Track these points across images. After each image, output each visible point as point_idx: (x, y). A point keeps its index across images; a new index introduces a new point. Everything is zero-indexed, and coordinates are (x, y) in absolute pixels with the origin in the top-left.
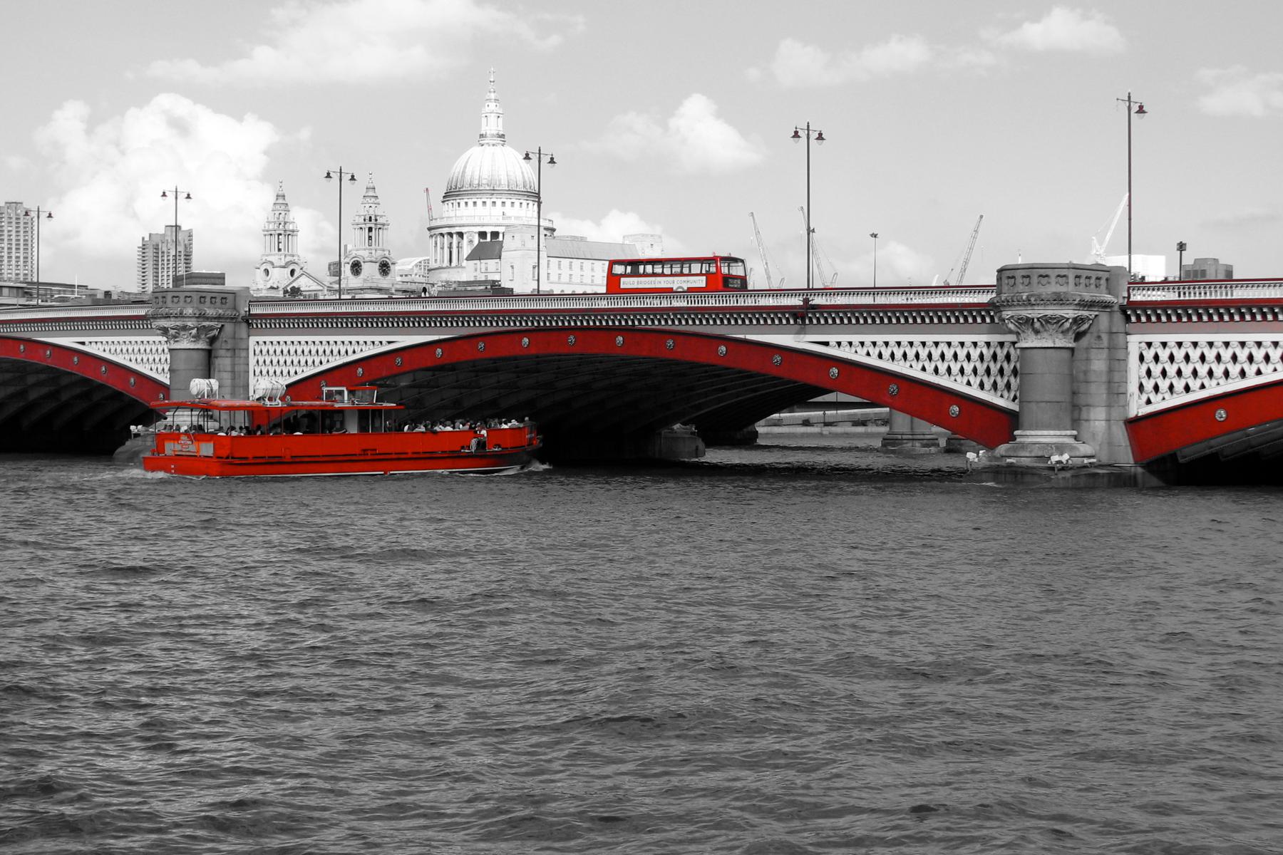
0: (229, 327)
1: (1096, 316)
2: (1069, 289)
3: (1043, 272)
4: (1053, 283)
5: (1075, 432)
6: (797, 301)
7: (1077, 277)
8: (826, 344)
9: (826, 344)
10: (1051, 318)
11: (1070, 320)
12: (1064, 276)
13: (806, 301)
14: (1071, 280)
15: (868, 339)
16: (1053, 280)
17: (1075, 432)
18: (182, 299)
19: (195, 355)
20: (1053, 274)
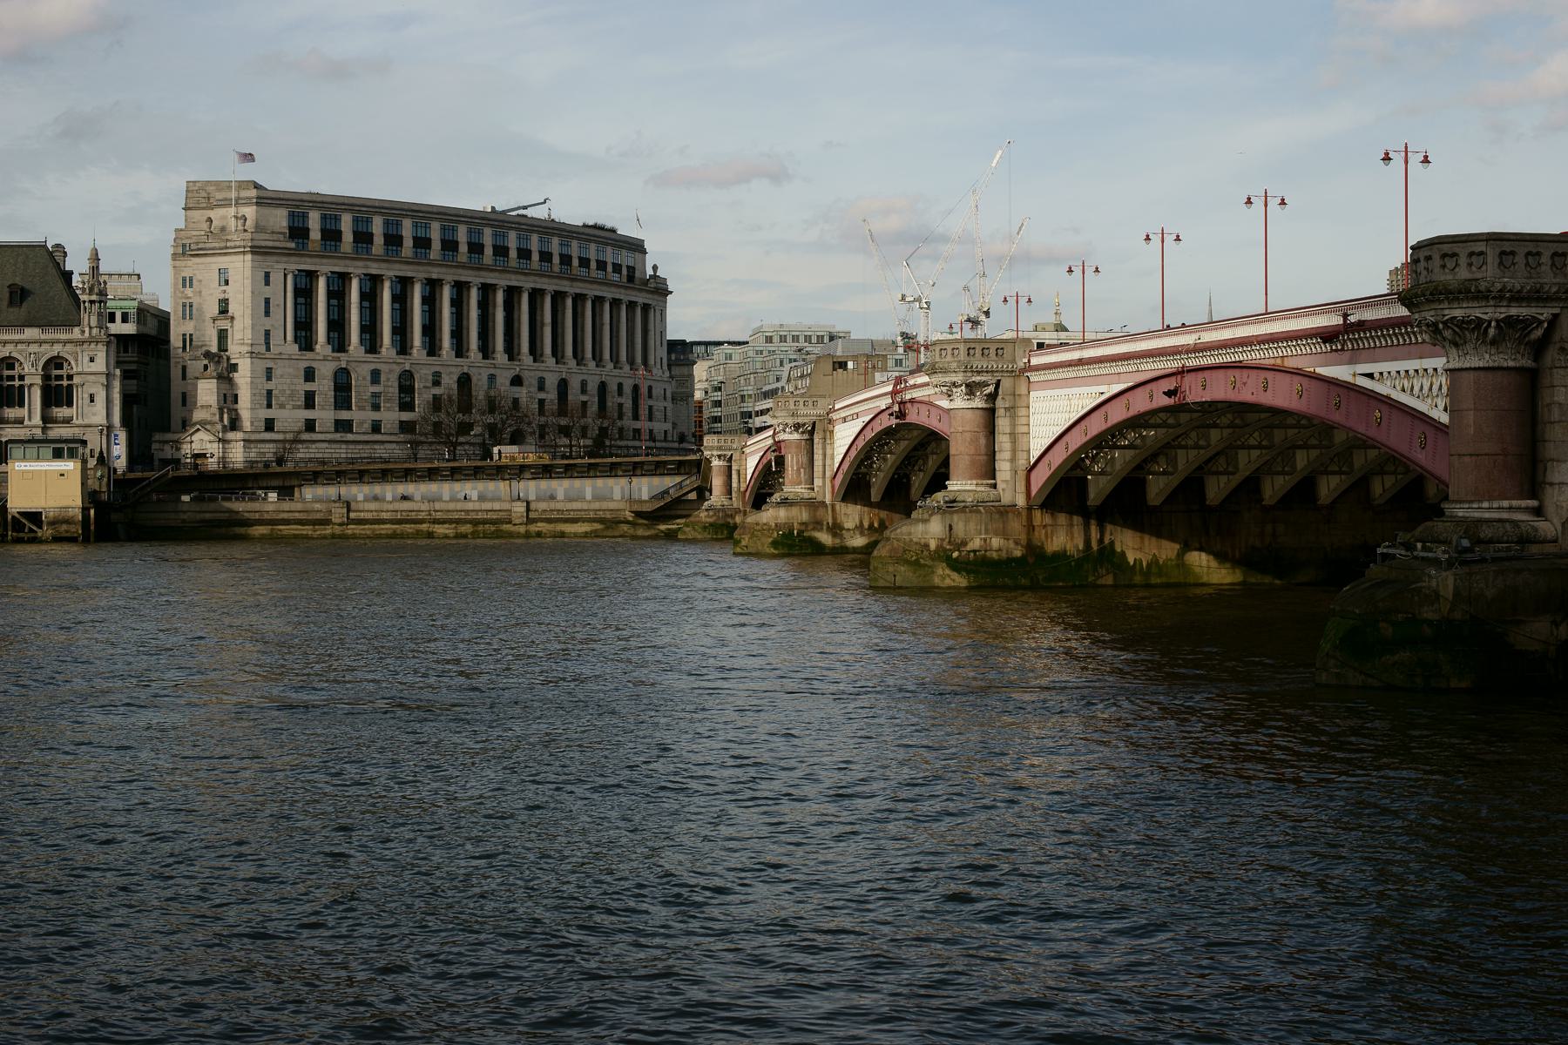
0: (1006, 384)
1: (1556, 316)
2: (1489, 273)
3: (1446, 248)
4: (1545, 268)
5: (1533, 503)
6: (1336, 320)
7: (1503, 253)
8: (1370, 376)
9: (1370, 376)
10: (1463, 322)
11: (1493, 324)
12: (1481, 253)
13: (1345, 316)
14: (1492, 258)
15: (1402, 365)
16: (1463, 260)
17: (1533, 503)
18: (949, 352)
19: (969, 414)
20: (1463, 251)
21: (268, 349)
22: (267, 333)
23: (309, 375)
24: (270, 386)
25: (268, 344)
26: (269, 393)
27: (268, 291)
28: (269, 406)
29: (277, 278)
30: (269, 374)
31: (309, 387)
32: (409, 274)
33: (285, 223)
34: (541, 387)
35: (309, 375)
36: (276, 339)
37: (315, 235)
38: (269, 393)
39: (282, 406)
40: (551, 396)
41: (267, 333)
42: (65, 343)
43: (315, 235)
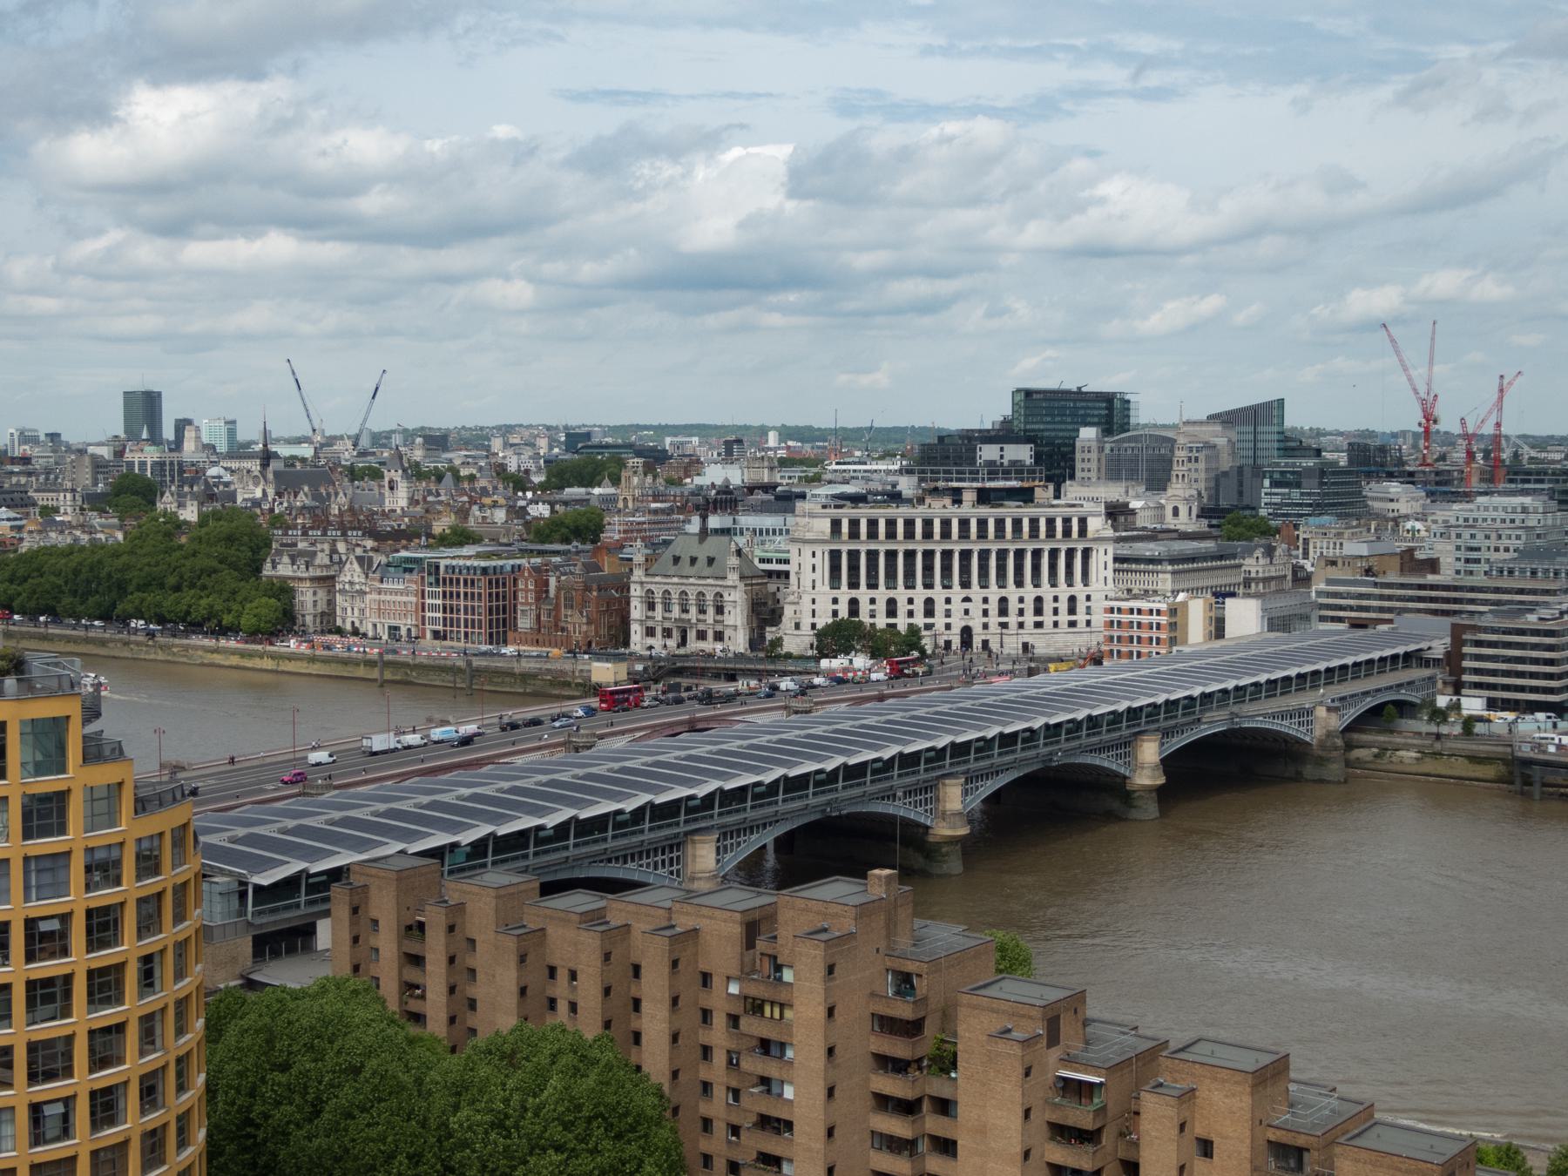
21: (814, 588)
22: (814, 581)
23: (835, 601)
24: (814, 607)
25: (814, 588)
26: (814, 611)
27: (813, 561)
28: (814, 616)
29: (819, 554)
30: (814, 601)
31: (835, 607)
32: (895, 548)
33: (829, 525)
34: (985, 600)
35: (835, 601)
36: (818, 584)
37: (845, 528)
38: (814, 611)
39: (820, 617)
40: (993, 607)
41: (814, 581)
42: (721, 586)
43: (845, 528)
